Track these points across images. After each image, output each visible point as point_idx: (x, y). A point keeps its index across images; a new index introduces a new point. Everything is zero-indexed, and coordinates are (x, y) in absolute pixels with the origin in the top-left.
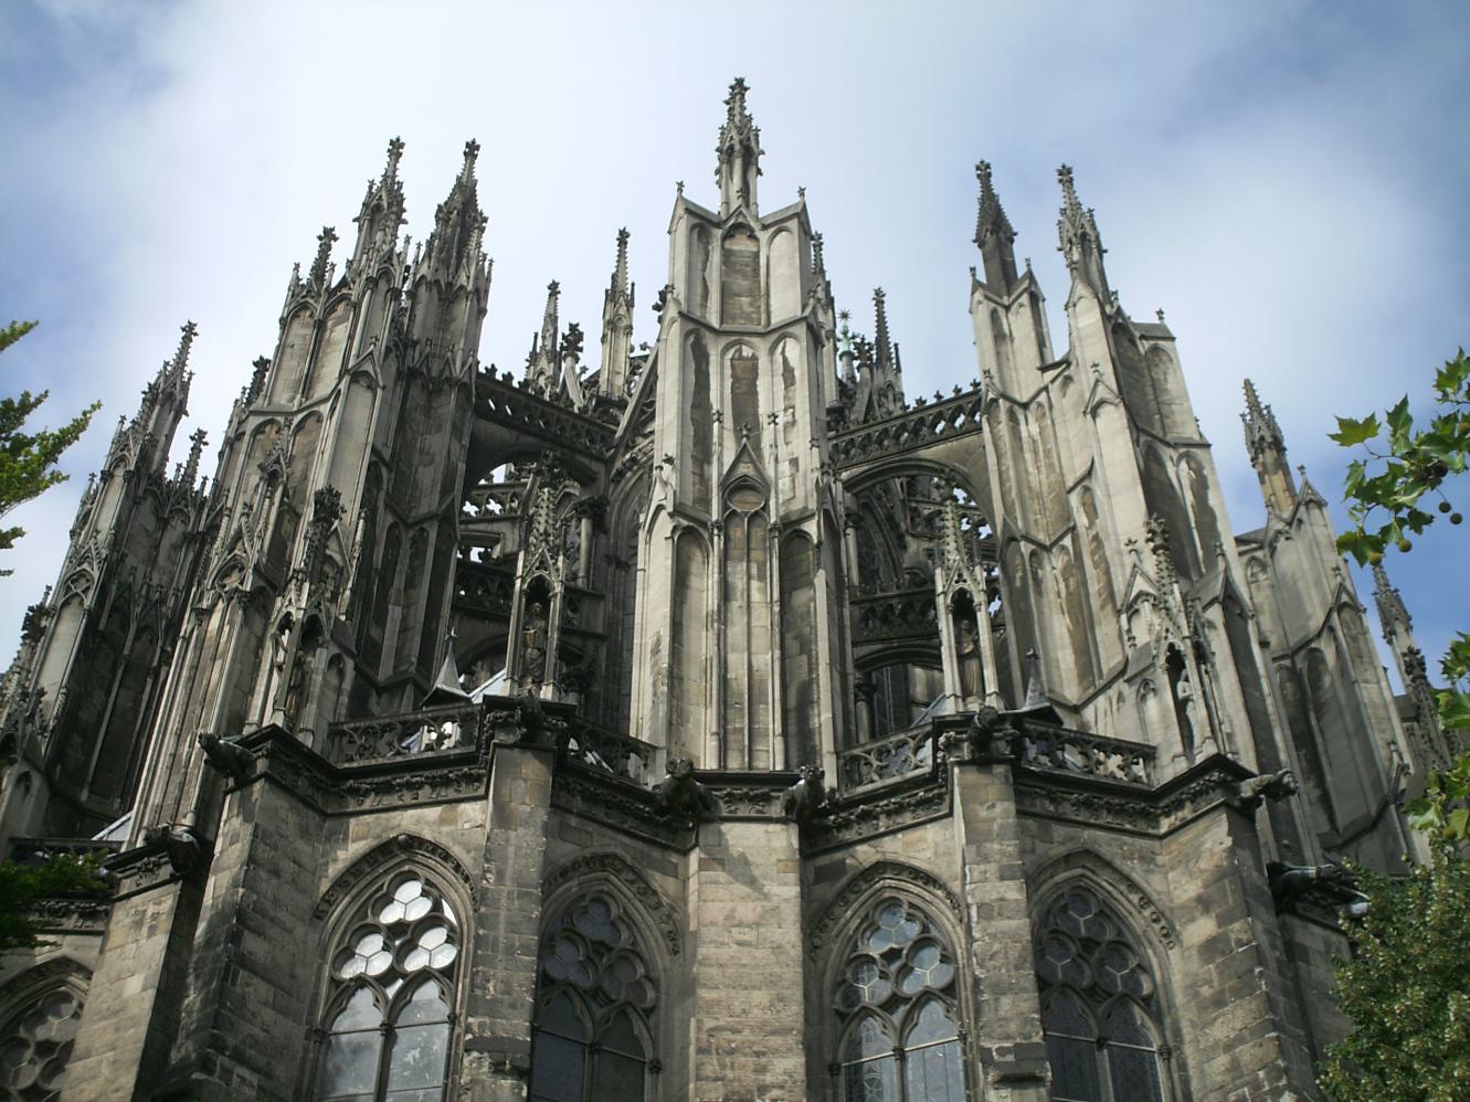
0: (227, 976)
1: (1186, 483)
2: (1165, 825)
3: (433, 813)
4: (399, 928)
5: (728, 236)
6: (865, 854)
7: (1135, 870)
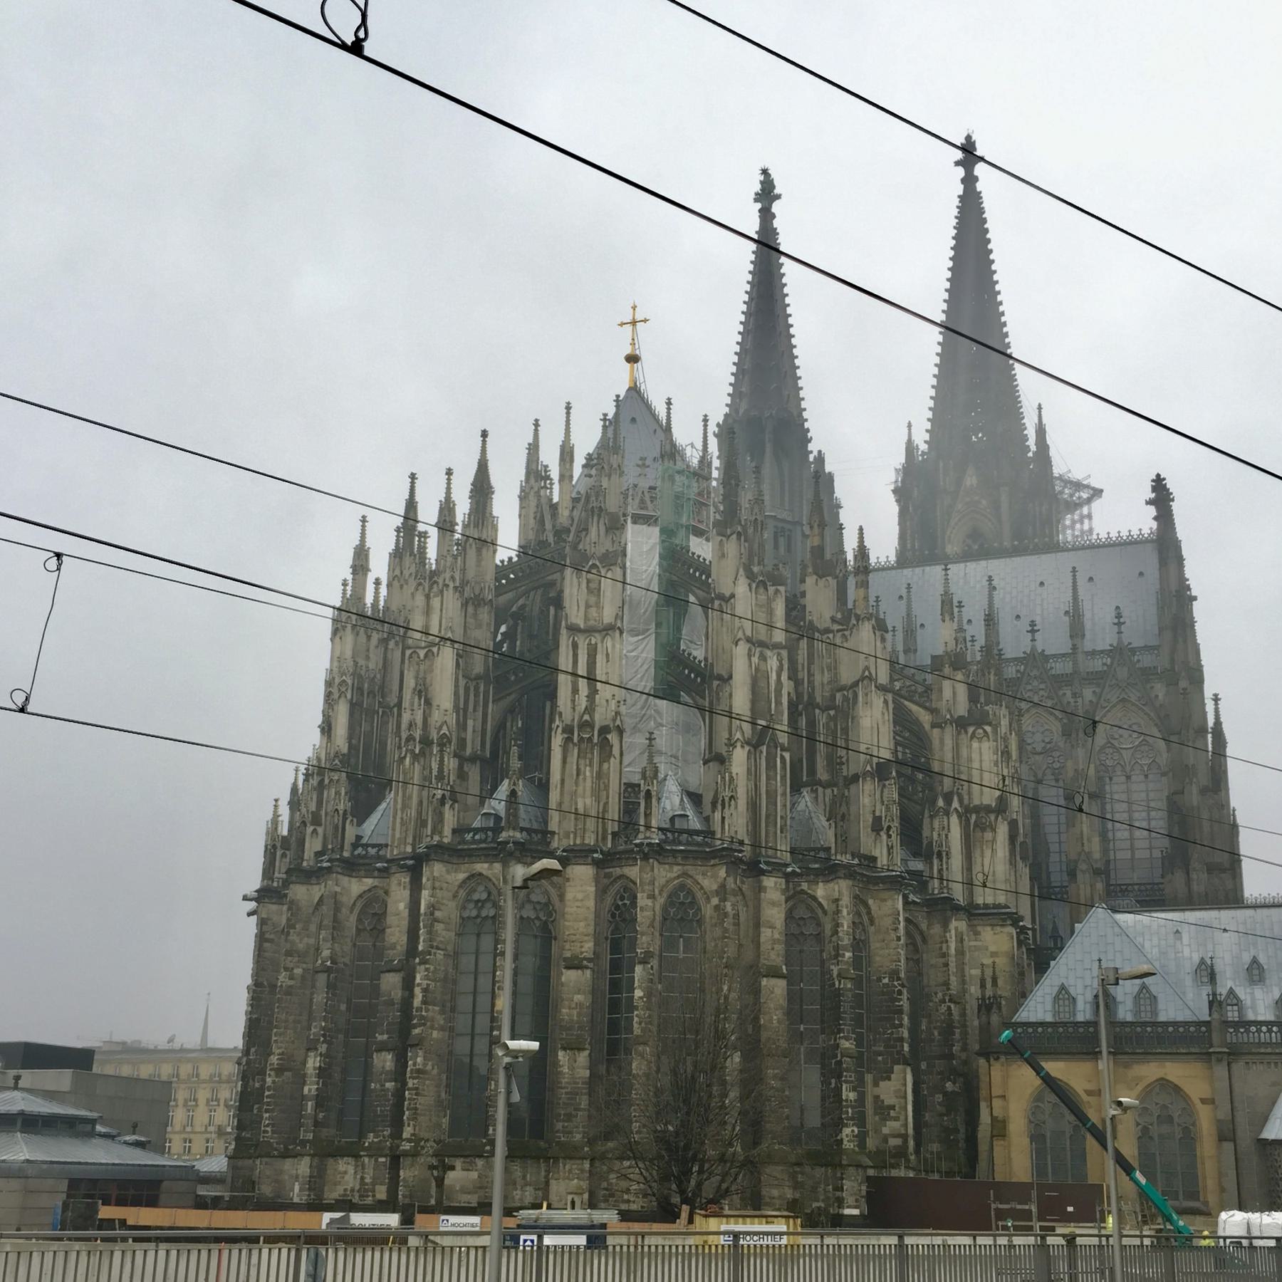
0: (432, 926)
1: (775, 668)
2: (712, 862)
3: (486, 865)
4: (479, 901)
6: (618, 871)
7: (700, 878)
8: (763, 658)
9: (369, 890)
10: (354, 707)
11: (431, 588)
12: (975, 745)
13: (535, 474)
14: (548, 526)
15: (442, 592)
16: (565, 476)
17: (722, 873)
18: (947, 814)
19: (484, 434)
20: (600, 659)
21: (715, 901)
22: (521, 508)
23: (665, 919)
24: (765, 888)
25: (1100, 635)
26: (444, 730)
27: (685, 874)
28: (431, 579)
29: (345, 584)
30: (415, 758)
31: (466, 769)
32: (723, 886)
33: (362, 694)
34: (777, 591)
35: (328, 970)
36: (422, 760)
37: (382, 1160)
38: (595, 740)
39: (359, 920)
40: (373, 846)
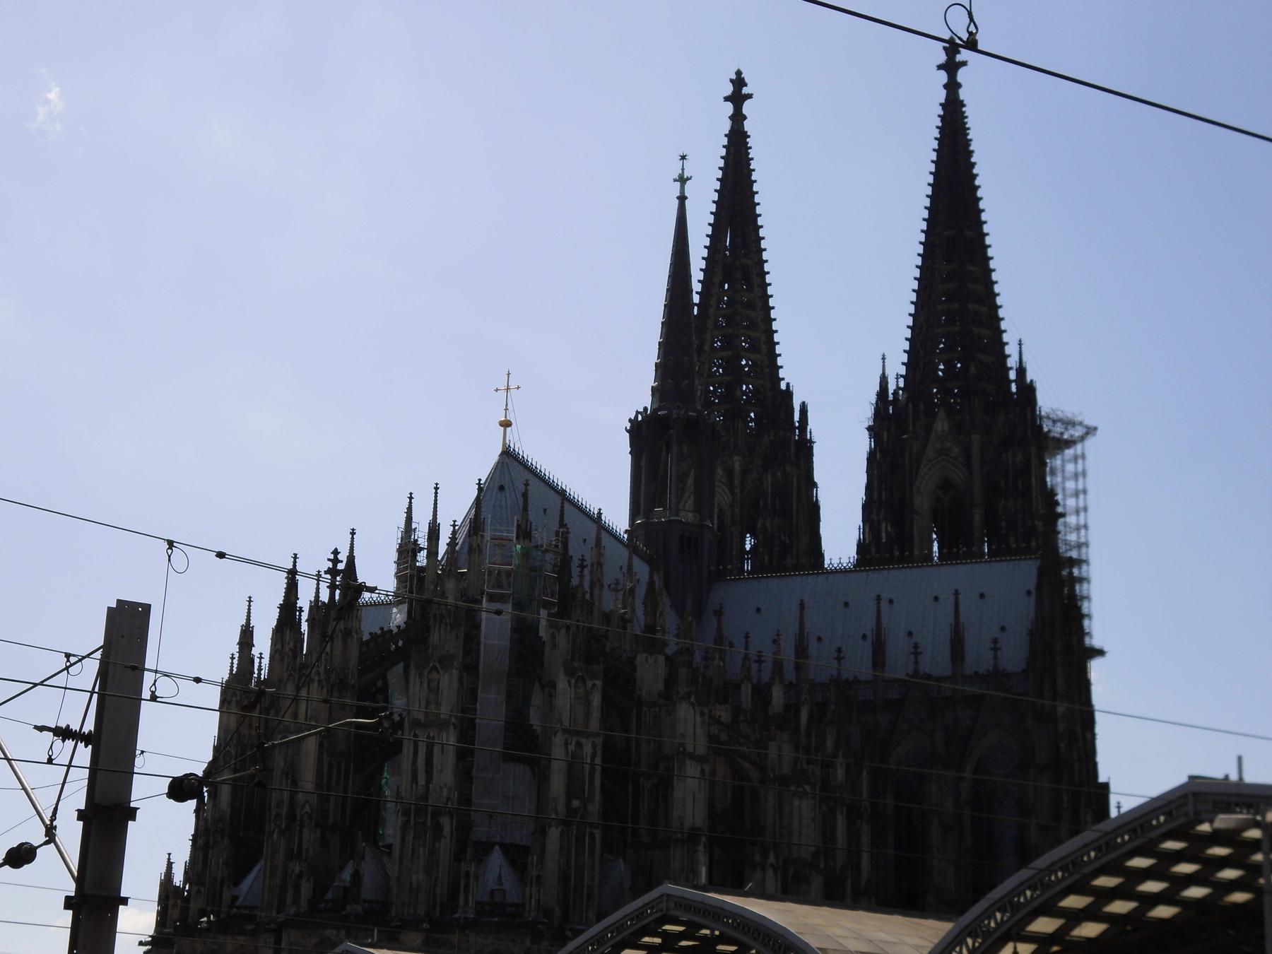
3: (334, 932)
5: (430, 672)
8: (579, 745)
12: (796, 802)
13: (407, 549)
16: (432, 552)
17: (528, 943)
18: (763, 869)
19: (353, 533)
20: (436, 749)
25: (978, 658)
29: (233, 658)
34: (594, 685)
38: (429, 823)
40: (246, 908)
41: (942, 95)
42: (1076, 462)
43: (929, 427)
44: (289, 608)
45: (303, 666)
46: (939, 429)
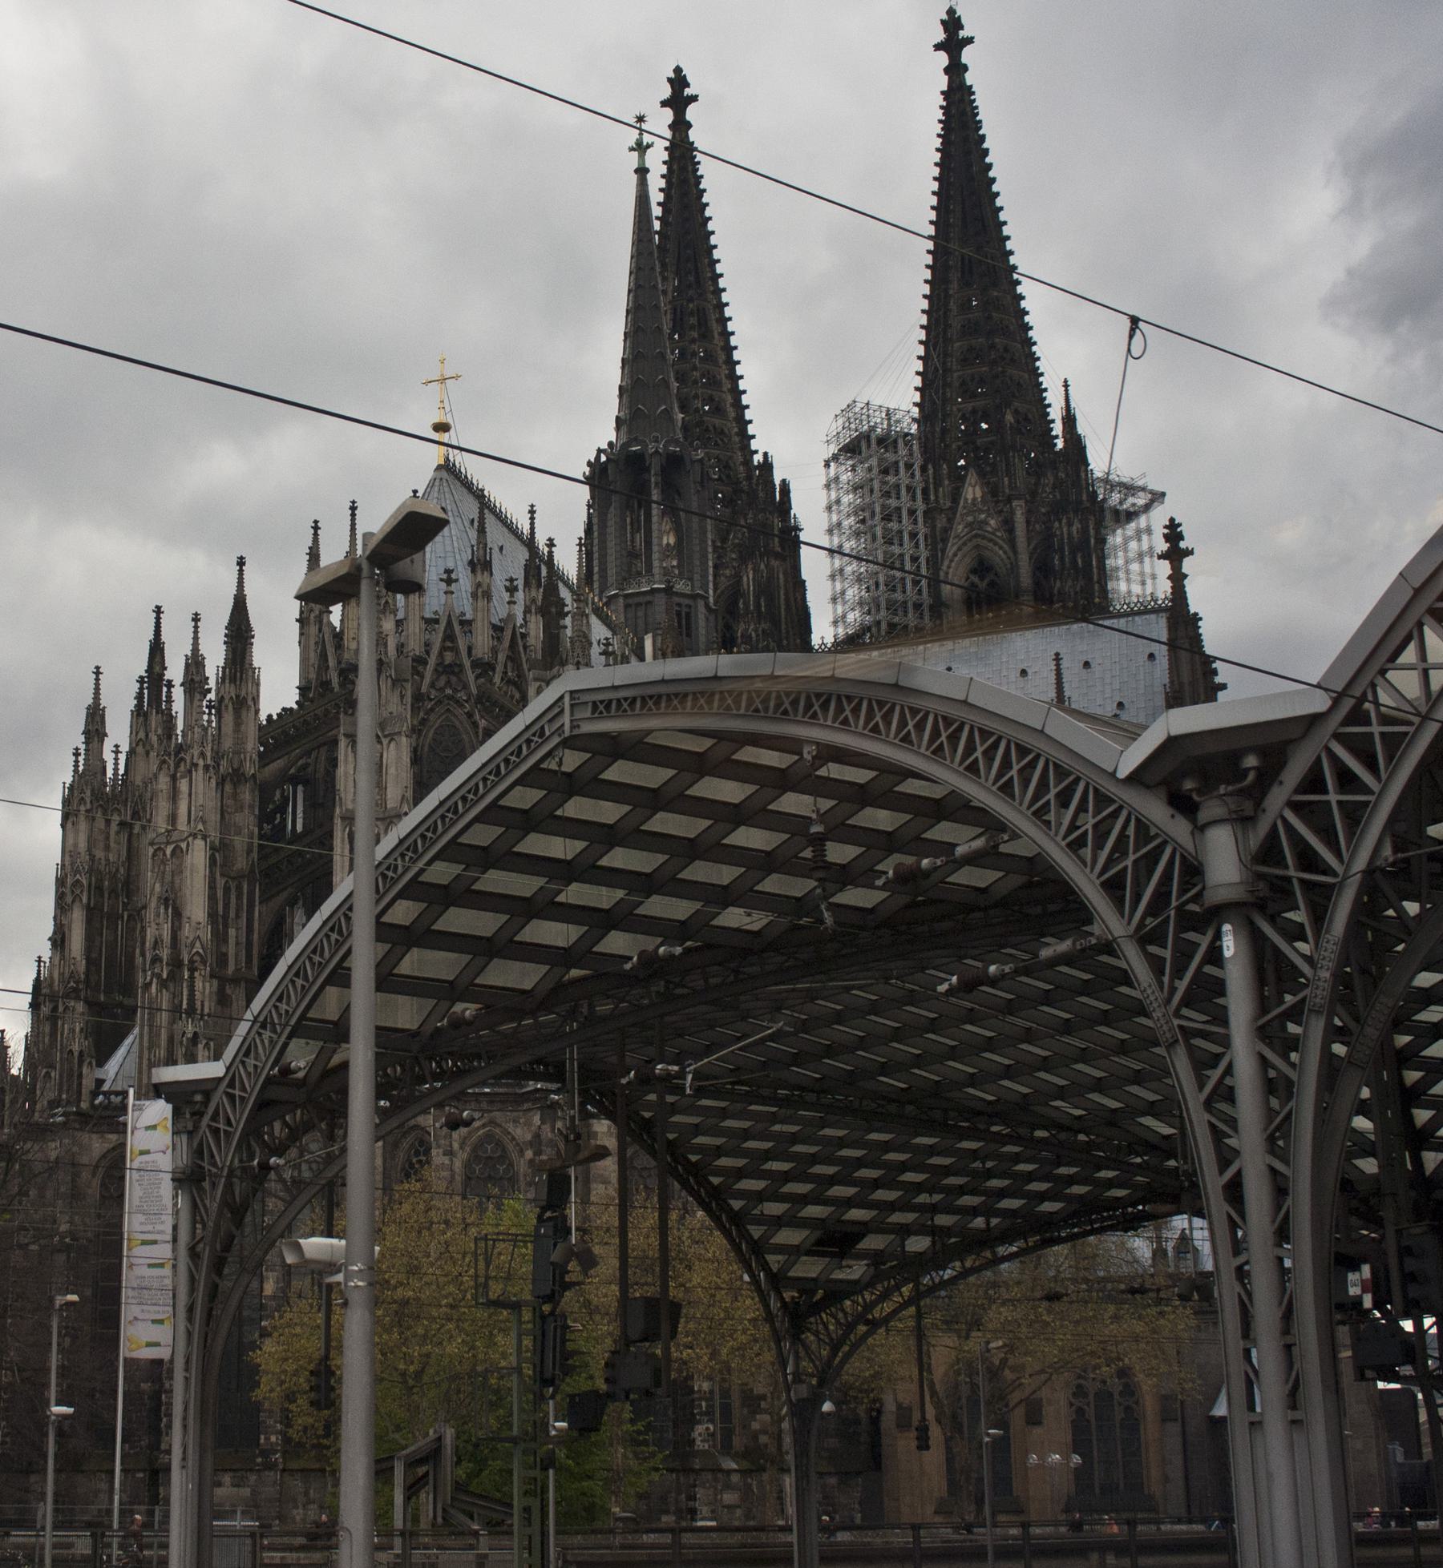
2: (526, 1106)
7: (510, 1127)
9: (114, 1149)
10: (91, 912)
11: (177, 766)
14: (332, 662)
15: (190, 772)
17: (537, 1119)
21: (529, 1154)
22: (301, 634)
23: (469, 1178)
24: (596, 1133)
26: (198, 948)
27: (492, 1122)
28: (176, 755)
29: (77, 754)
30: (163, 984)
31: (228, 991)
32: (537, 1136)
33: (102, 896)
35: (68, 1249)
36: (171, 985)
37: (141, 1475)
39: (103, 1185)
41: (943, 82)
42: (1139, 540)
43: (956, 496)
44: (154, 678)
45: (180, 748)
46: (970, 496)
